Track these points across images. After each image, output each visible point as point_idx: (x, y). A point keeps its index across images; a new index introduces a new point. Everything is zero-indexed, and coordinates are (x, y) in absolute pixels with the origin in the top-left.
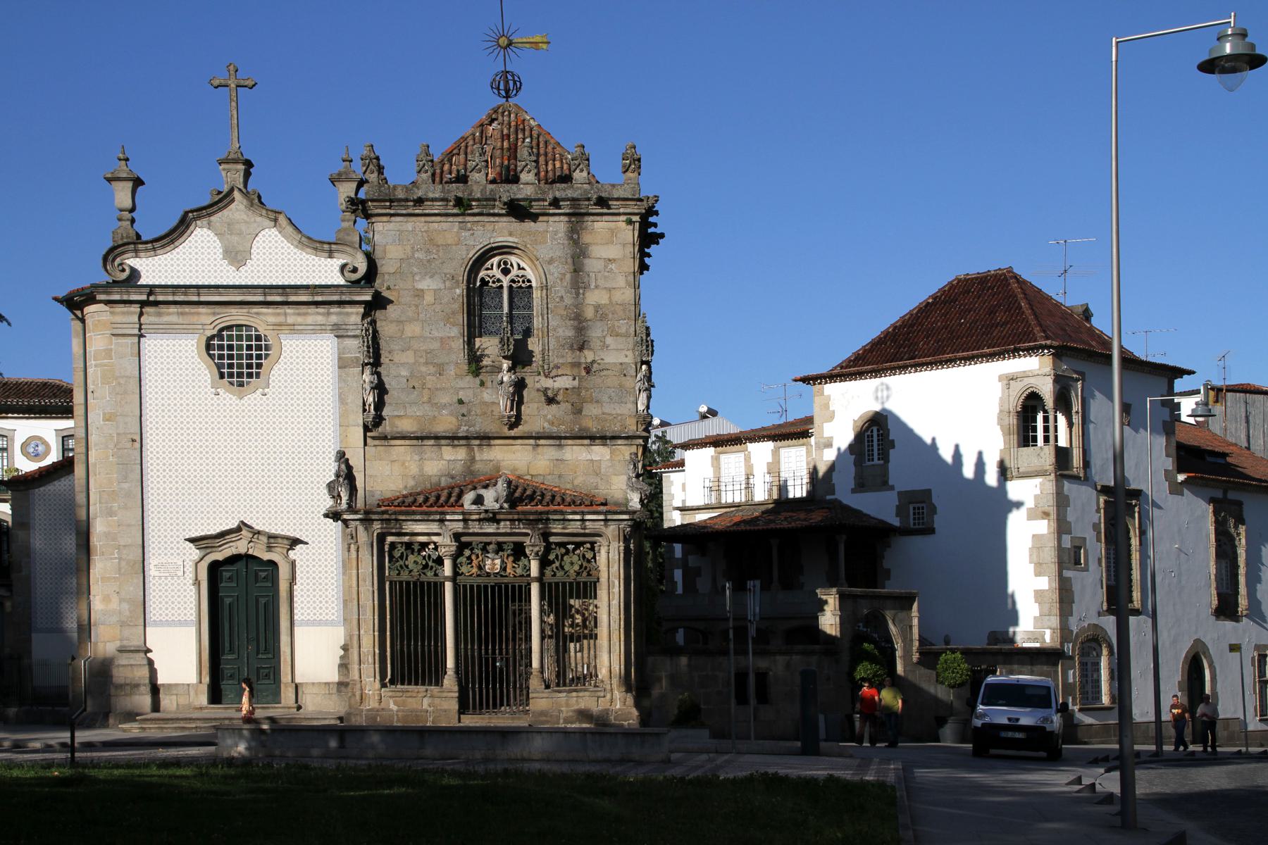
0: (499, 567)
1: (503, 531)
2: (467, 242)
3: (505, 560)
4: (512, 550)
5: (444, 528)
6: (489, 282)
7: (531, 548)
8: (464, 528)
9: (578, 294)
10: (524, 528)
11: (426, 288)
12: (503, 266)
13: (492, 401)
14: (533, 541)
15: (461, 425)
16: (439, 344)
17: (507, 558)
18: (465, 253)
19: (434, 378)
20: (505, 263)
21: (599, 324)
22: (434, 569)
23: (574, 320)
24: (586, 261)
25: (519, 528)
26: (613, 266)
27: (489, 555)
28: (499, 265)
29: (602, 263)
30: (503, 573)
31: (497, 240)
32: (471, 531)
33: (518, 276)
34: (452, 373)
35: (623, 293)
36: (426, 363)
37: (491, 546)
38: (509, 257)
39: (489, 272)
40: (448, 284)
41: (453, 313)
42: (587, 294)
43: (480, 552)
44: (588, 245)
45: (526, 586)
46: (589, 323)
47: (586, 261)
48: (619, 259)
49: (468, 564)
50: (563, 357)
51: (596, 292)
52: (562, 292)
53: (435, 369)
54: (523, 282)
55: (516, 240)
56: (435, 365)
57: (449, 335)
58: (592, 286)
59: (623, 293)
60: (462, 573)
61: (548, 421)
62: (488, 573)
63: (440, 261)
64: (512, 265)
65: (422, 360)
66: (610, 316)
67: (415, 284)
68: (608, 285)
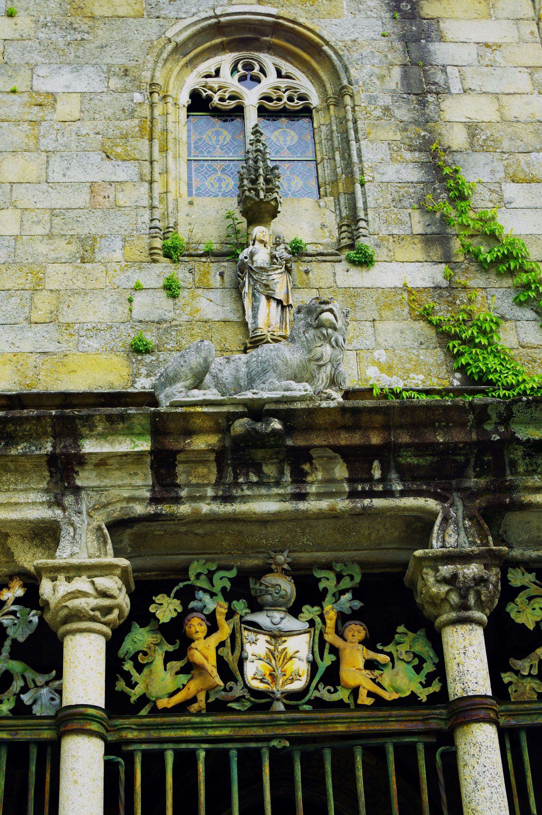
0: (304, 668)
1: (324, 504)
2: (163, 13)
3: (331, 637)
4: (357, 593)
5: (69, 500)
6: (209, 99)
7: (446, 570)
8: (154, 500)
9: (423, 104)
10: (404, 494)
11: (59, 90)
12: (242, 71)
13: (221, 317)
14: (451, 540)
15: (136, 375)
16: (87, 198)
17: (339, 633)
18: (156, 29)
19: (68, 268)
20: (248, 67)
21: (481, 158)
22: (17, 685)
23: (420, 151)
24: (435, 47)
25: (387, 494)
26: (498, 56)
27: (261, 618)
28: (234, 69)
29: (473, 50)
30: (324, 694)
31: (231, 10)
32: (184, 509)
33: (278, 88)
34: (118, 255)
35: (527, 103)
36: (50, 236)
37: (270, 579)
38: (256, 54)
39: (209, 80)
40: (114, 83)
41: (125, 137)
42: (447, 104)
43: (222, 608)
44: (437, 20)
45: (430, 750)
46: (458, 157)
47: (435, 47)
48: (507, 44)
49: (168, 658)
50: (401, 222)
51: (466, 99)
52: (386, 100)
53: (73, 248)
54: (290, 99)
55: (273, 11)
56: (70, 239)
57: (114, 179)
58: (455, 87)
59: (527, 103)
60: (144, 700)
61: (379, 364)
62: (255, 693)
63: (98, 43)
64: (262, 70)
65: (39, 230)
66: (506, 145)
67: (35, 83)
68: (490, 90)
